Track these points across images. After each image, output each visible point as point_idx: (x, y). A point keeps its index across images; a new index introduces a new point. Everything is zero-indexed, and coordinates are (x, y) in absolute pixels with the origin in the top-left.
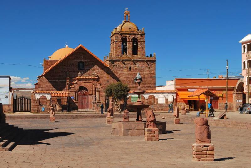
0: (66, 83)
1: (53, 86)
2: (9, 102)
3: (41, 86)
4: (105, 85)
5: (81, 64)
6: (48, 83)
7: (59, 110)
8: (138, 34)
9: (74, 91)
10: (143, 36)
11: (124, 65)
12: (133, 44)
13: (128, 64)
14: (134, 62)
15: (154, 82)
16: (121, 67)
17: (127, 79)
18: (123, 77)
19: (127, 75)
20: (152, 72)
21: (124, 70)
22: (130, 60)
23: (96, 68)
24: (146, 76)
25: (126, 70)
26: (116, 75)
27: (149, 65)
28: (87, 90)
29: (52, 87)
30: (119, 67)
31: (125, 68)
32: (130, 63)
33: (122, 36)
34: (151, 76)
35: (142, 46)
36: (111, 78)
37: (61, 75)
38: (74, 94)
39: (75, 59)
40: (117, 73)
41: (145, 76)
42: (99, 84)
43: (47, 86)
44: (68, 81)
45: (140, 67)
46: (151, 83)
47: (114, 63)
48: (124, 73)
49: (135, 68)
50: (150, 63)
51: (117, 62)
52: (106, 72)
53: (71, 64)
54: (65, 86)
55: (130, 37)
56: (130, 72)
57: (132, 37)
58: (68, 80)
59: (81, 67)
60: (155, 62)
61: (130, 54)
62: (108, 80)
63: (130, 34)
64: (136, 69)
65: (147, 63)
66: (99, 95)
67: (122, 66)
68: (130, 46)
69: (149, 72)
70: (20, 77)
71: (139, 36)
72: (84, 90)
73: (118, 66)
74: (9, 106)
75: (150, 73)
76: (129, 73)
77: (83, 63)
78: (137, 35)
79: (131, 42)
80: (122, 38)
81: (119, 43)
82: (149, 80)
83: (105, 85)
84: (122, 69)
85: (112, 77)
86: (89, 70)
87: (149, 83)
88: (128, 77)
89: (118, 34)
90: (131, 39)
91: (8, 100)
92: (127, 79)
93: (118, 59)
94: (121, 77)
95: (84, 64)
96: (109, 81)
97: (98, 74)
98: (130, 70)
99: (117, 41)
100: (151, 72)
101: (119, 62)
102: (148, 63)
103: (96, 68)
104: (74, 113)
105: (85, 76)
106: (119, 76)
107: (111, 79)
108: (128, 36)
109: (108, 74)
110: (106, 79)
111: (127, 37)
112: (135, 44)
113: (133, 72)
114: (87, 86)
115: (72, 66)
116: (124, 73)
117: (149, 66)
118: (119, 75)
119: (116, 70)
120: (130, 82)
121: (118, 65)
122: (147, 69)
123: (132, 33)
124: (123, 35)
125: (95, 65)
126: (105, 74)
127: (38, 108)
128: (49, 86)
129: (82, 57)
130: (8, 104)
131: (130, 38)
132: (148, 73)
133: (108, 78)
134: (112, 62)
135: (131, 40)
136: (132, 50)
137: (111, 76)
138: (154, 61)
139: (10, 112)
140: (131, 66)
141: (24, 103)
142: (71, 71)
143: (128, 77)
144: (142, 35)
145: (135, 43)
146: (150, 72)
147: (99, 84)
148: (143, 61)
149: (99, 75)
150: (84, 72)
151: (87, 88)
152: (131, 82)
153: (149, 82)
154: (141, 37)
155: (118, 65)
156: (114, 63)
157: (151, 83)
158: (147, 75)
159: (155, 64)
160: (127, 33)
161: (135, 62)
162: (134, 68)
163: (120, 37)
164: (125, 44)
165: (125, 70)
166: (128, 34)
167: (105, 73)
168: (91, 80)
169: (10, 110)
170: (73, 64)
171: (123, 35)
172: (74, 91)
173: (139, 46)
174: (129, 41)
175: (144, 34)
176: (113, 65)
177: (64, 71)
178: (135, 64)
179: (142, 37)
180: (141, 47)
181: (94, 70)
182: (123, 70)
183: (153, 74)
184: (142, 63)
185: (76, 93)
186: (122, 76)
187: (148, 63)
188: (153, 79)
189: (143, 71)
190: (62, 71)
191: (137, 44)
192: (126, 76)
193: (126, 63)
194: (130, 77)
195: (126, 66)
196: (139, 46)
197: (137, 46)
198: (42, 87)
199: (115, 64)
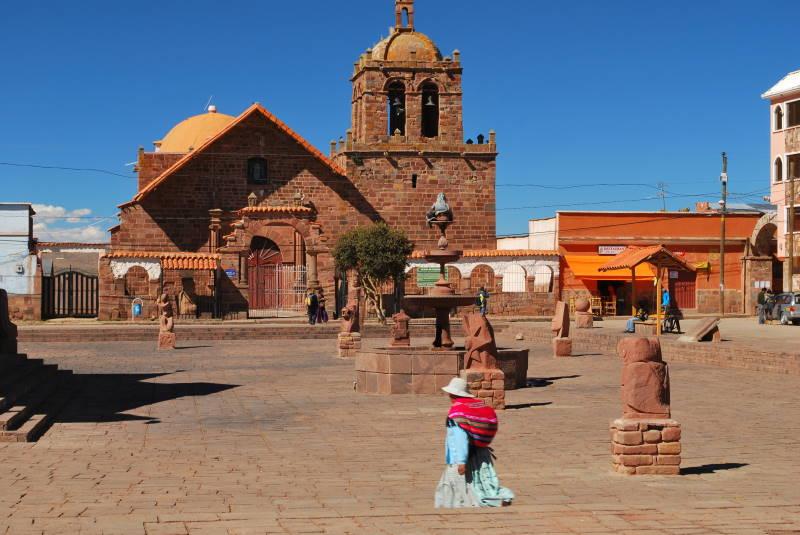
0: (211, 227)
1: (168, 235)
2: (29, 287)
3: (128, 235)
4: (333, 232)
5: (257, 167)
6: (153, 227)
7: (188, 313)
8: (440, 71)
9: (235, 253)
10: (454, 76)
11: (396, 170)
12: (425, 101)
13: (407, 165)
14: (426, 160)
15: (489, 223)
16: (385, 177)
18: (391, 207)
19: (405, 200)
20: (485, 192)
21: (395, 186)
22: (415, 154)
23: (305, 178)
24: (466, 204)
25: (401, 187)
26: (370, 199)
27: (473, 169)
28: (276, 248)
29: (165, 237)
30: (380, 176)
31: (399, 177)
32: (413, 163)
33: (387, 76)
34: (482, 205)
35: (451, 109)
36: (354, 210)
37: (194, 201)
38: (236, 262)
39: (238, 148)
40: (373, 195)
41: (461, 204)
42: (314, 228)
43: (149, 236)
44: (217, 220)
45: (446, 177)
46: (479, 228)
47: (362, 164)
48: (393, 196)
49: (431, 177)
50: (477, 163)
51: (373, 161)
52: (338, 192)
53: (225, 166)
54: (206, 238)
55: (413, 78)
56: (412, 191)
57: (421, 79)
58: (215, 217)
59: (257, 176)
60: (493, 159)
61: (414, 134)
62: (343, 217)
63: (414, 71)
65: (468, 162)
66: (316, 264)
67: (387, 172)
68: (413, 107)
70: (63, 206)
71: (443, 77)
72: (266, 248)
73: (377, 172)
74: (27, 298)
76: (411, 195)
77: (262, 161)
78: (436, 74)
79: (416, 95)
80: (388, 82)
81: (380, 99)
82: (476, 218)
83: (333, 232)
84: (389, 181)
85: (357, 208)
86: (284, 184)
87: (473, 228)
89: (377, 69)
90: (416, 87)
91: (23, 279)
92: (405, 214)
93: (375, 150)
95: (266, 168)
96: (348, 219)
97: (311, 199)
98: (414, 186)
99: (372, 94)
100: (480, 191)
101: (379, 161)
102: (472, 162)
103: (305, 178)
104: (236, 322)
105: (272, 204)
106: (378, 204)
107: (352, 214)
108: (407, 75)
109: (344, 196)
110: (338, 213)
111: (404, 78)
112: (430, 103)
113: (424, 191)
114: (278, 234)
115: (228, 171)
116: (393, 196)
117: (474, 173)
118: (380, 200)
119: (369, 184)
120: (412, 224)
121: (374, 169)
122: (468, 182)
123: (419, 66)
124: (393, 75)
125: (302, 169)
126: (335, 199)
127: (121, 306)
128: (157, 236)
129: (262, 143)
130: (25, 291)
131: (413, 84)
132: (470, 195)
133: (343, 209)
134: (355, 160)
135: (419, 89)
136: (420, 122)
137: (352, 204)
138: (490, 158)
139: (30, 317)
140: (417, 172)
141: (74, 288)
142: (226, 190)
144: (454, 73)
145: (430, 98)
146: (477, 191)
147: (314, 228)
148: (456, 156)
149: (314, 202)
150: (266, 191)
151: (275, 241)
152: (416, 223)
154: (449, 80)
155: (374, 169)
156: (362, 164)
157: (479, 228)
158: (468, 200)
159: (494, 165)
160: (403, 65)
161: (429, 159)
162: (428, 180)
163: (381, 81)
164: (397, 102)
165: (398, 185)
166: (407, 70)
167: (334, 193)
168: (290, 217)
169: (30, 312)
170: (233, 166)
171: (393, 75)
172: (235, 253)
173: (443, 109)
174: (410, 91)
175: (460, 71)
176: (360, 168)
177: (205, 189)
178: (431, 167)
179: (453, 79)
180: (449, 112)
181: (300, 183)
182: (392, 186)
183: (487, 196)
184: (452, 163)
185: (243, 259)
186: (389, 204)
187: (472, 162)
188: (487, 214)
189: (454, 187)
190: (196, 189)
191: (436, 101)
193: (401, 162)
196: (443, 109)
197: (435, 109)
198: (133, 240)
199: (367, 165)
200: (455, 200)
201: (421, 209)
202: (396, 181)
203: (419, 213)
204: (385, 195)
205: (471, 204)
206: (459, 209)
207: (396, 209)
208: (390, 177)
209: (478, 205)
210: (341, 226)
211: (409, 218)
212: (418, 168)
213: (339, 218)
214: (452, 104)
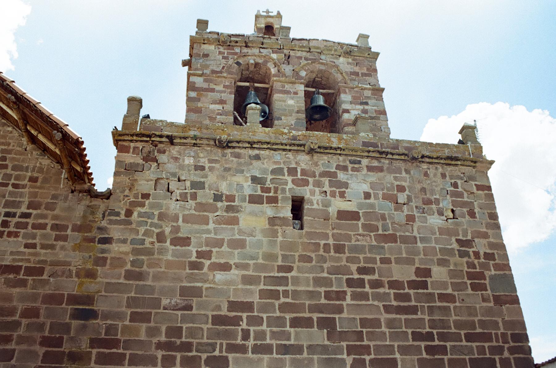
4: (45, 342)
15: (508, 324)
16: (218, 198)
17: (275, 295)
18: (235, 273)
31: (254, 200)
41: (427, 273)
46: (486, 337)
62: (89, 299)
64: (343, 215)
69: (455, 246)
75: (463, 254)
76: (289, 246)
82: (471, 311)
83: (45, 342)
84: (229, 209)
87: (470, 338)
88: (283, 281)
92: (275, 295)
94: (219, 276)
118: (200, 254)
143: (283, 281)
152: (308, 323)
153: (472, 325)
157: (486, 337)
158: (442, 263)
162: (332, 210)
182: (235, 221)
183: (488, 256)
186: (226, 267)
188: (498, 301)
192: (258, 267)
194: (296, 281)
195: (268, 190)
200: (409, 261)
201: (318, 281)
202: (249, 207)
203: (312, 295)
204: (219, 243)
205: (453, 274)
206: (424, 285)
207: (247, 280)
208: (230, 198)
209: (471, 276)
210: (75, 323)
211: (284, 308)
212: (306, 183)
213: (73, 299)
214: (366, 104)
